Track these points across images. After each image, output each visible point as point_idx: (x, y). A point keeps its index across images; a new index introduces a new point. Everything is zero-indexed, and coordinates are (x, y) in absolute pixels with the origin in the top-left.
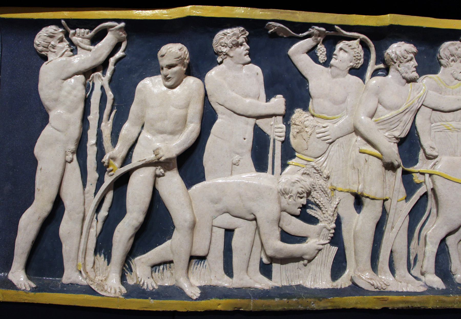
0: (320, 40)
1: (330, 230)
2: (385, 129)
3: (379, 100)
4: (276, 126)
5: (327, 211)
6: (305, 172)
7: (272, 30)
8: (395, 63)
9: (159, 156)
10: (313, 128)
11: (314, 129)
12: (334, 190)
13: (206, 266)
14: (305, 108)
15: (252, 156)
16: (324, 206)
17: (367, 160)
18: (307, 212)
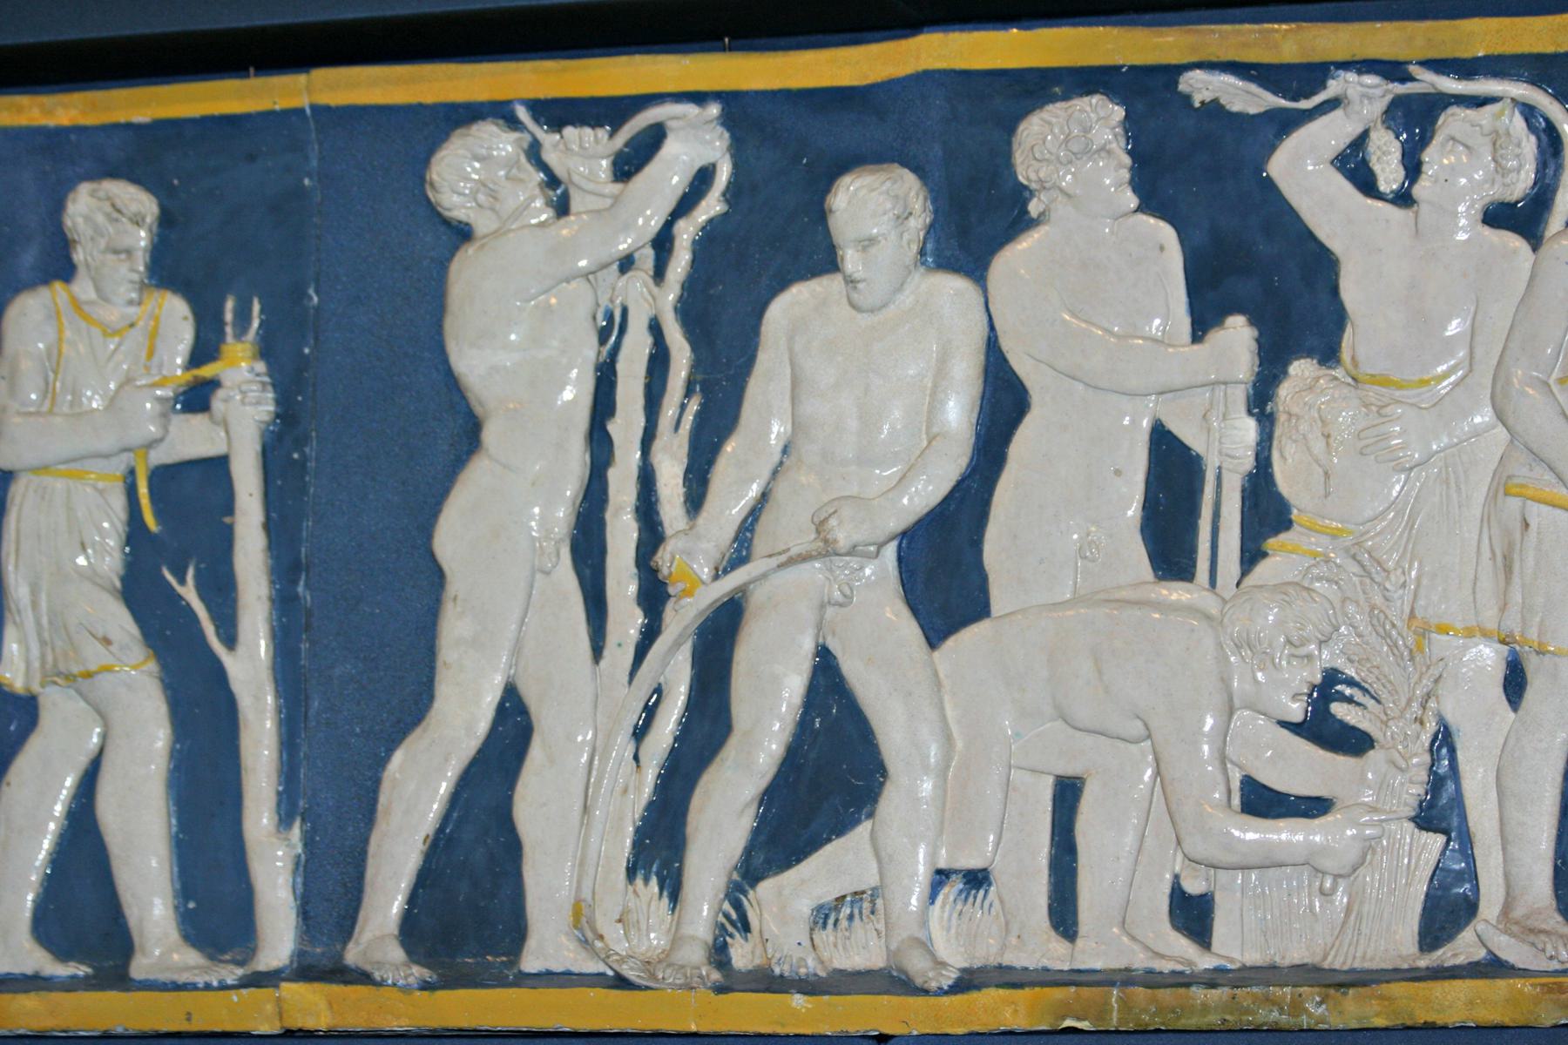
13: (991, 905)
14: (1329, 355)
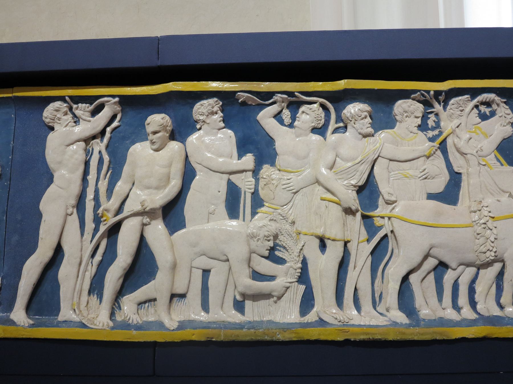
0: (285, 105)
1: (296, 270)
2: (343, 178)
3: (336, 154)
4: (246, 180)
5: (293, 252)
6: (272, 218)
7: (241, 100)
8: (351, 121)
9: (144, 207)
10: (278, 180)
11: (279, 181)
12: (300, 234)
13: (186, 303)
14: (273, 164)
15: (226, 207)
16: (290, 248)
17: (327, 206)
18: (275, 254)
